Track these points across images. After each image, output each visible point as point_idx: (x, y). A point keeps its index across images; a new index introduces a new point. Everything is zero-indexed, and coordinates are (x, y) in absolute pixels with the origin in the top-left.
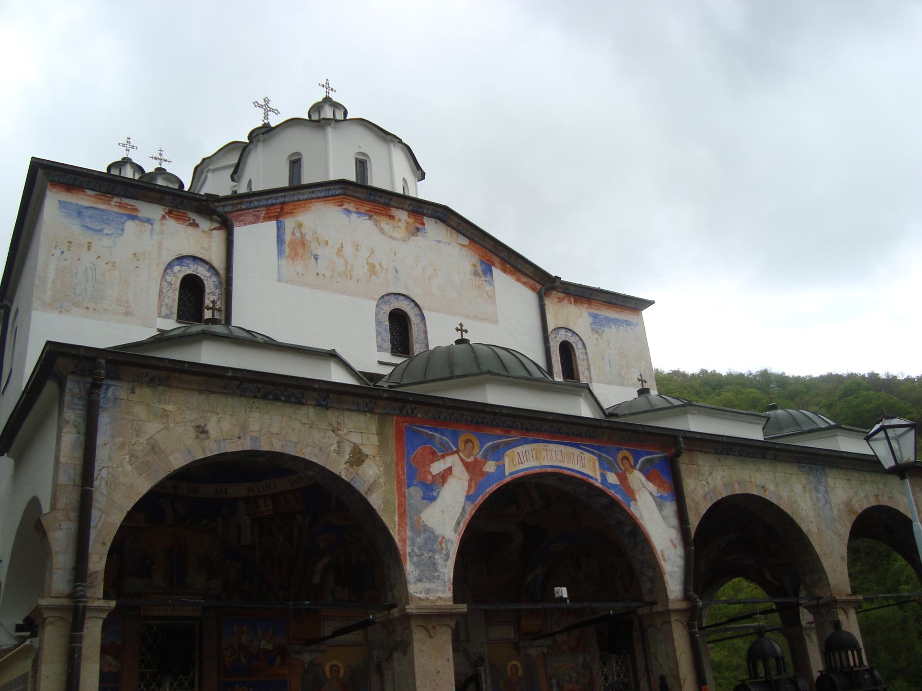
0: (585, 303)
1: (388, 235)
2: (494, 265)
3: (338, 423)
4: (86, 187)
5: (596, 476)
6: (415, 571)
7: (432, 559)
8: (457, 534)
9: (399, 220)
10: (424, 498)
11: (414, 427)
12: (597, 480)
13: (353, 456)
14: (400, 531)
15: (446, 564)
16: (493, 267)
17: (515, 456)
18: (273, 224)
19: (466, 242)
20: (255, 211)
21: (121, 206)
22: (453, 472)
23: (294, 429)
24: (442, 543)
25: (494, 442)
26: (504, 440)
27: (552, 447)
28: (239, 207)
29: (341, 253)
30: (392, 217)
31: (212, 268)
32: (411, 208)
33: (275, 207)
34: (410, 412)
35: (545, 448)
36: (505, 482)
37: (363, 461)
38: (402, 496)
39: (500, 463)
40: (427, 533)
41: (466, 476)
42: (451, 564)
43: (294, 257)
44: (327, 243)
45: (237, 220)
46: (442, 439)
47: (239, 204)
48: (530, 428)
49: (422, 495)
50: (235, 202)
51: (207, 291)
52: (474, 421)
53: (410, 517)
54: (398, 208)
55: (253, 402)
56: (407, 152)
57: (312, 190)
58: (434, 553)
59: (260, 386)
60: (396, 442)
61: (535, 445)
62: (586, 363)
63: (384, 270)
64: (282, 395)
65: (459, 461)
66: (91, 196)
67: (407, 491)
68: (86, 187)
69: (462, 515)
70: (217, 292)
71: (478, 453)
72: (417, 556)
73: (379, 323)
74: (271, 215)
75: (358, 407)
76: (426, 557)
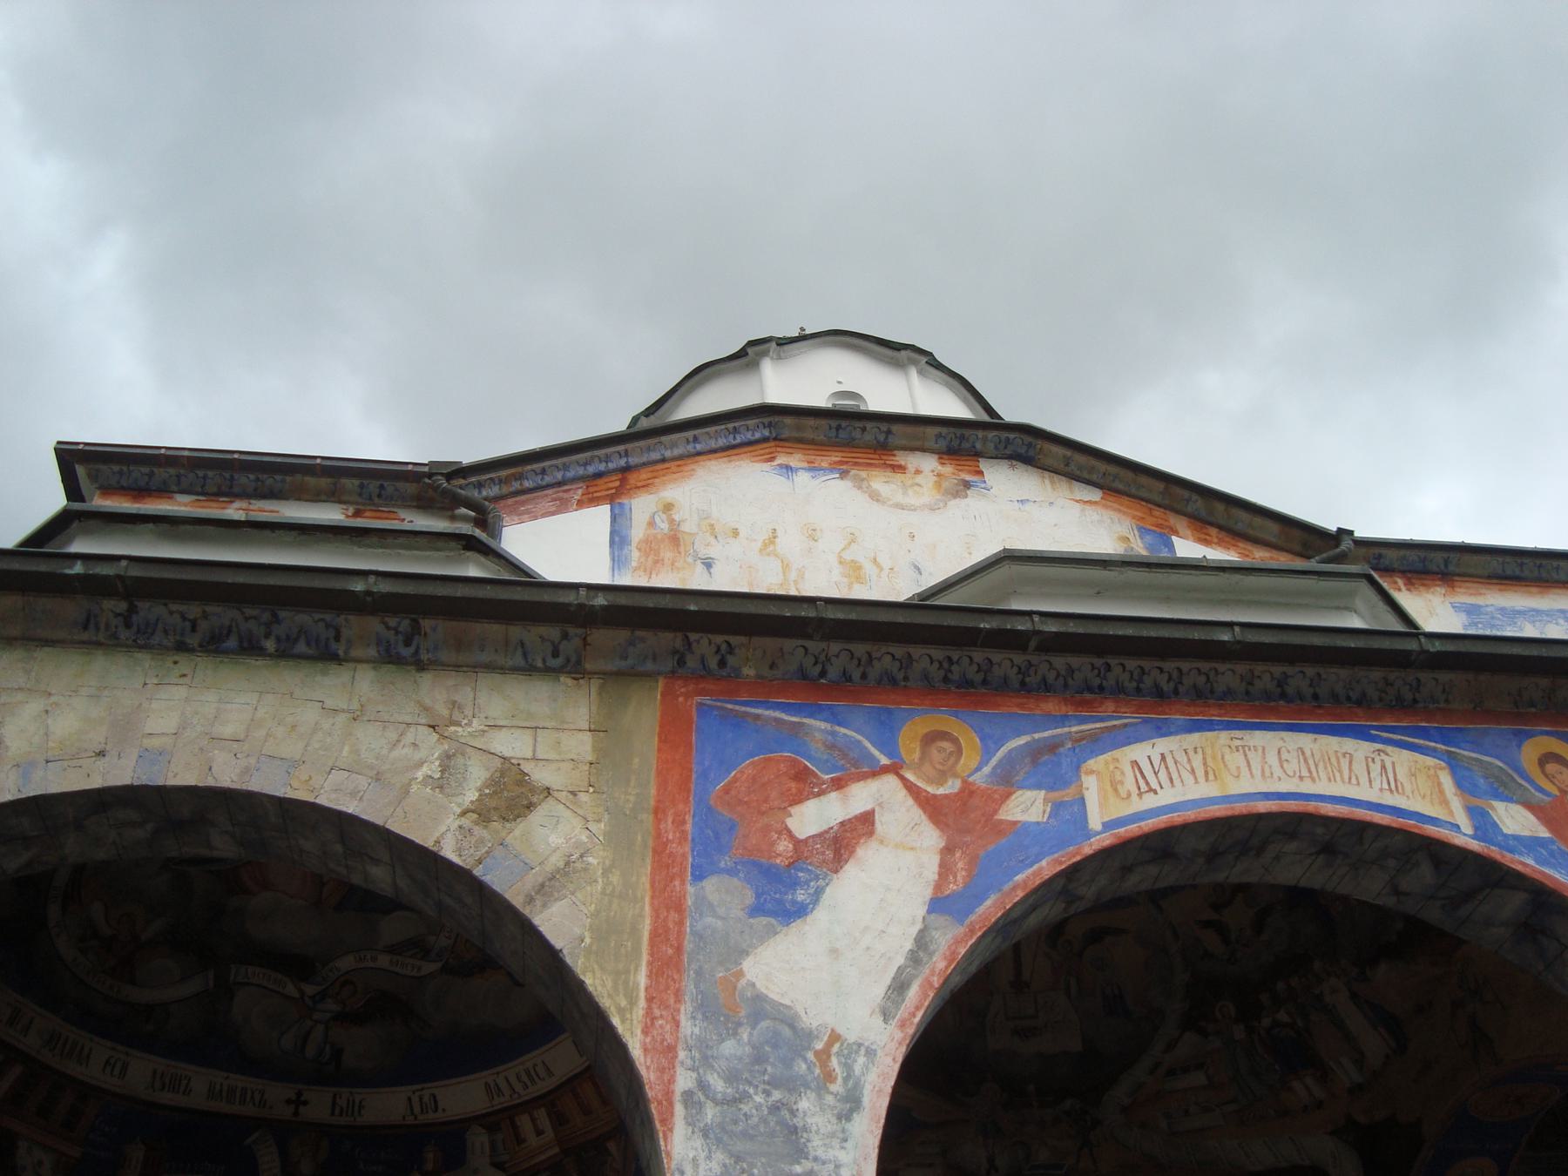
0: (1436, 585)
1: (891, 503)
2: (1176, 533)
3: (454, 704)
4: (176, 489)
5: (1451, 813)
6: (709, 1158)
7: (785, 1113)
8: (894, 1022)
9: (918, 472)
10: (756, 910)
11: (730, 706)
12: (1458, 827)
13: (495, 793)
14: (653, 1019)
15: (843, 1131)
16: (1174, 538)
17: (1123, 773)
18: (602, 513)
19: (1096, 495)
20: (558, 492)
22: (878, 825)
23: (294, 727)
24: (829, 1056)
25: (1036, 736)
26: (1074, 729)
27: (1259, 738)
28: (516, 485)
29: (771, 548)
32: (942, 444)
33: (605, 480)
34: (713, 663)
35: (1238, 743)
36: (1088, 850)
37: (530, 807)
38: (669, 905)
39: (1067, 794)
40: (764, 1024)
41: (931, 838)
42: (867, 1130)
44: (735, 533)
45: (513, 511)
46: (833, 734)
47: (516, 480)
48: (1167, 688)
49: (749, 897)
50: (504, 473)
52: (955, 676)
53: (699, 973)
54: (913, 449)
55: (175, 663)
56: (965, 392)
57: (690, 434)
58: (791, 1090)
59: (194, 610)
60: (659, 750)
61: (1195, 738)
63: (886, 571)
64: (267, 636)
65: (902, 794)
67: (690, 889)
68: (176, 489)
69: (915, 958)
71: (978, 769)
72: (716, 1103)
74: (595, 495)
75: (525, 655)
76: (758, 1107)
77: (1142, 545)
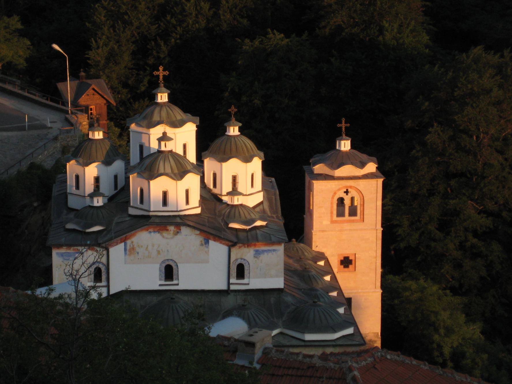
0: (253, 246)
2: (210, 239)
9: (171, 230)
18: (124, 243)
19: (198, 232)
21: (74, 250)
30: (167, 230)
31: (103, 264)
43: (130, 255)
44: (142, 246)
51: (102, 271)
62: (249, 271)
66: (65, 249)
70: (105, 271)
73: (160, 271)
77: (204, 242)
